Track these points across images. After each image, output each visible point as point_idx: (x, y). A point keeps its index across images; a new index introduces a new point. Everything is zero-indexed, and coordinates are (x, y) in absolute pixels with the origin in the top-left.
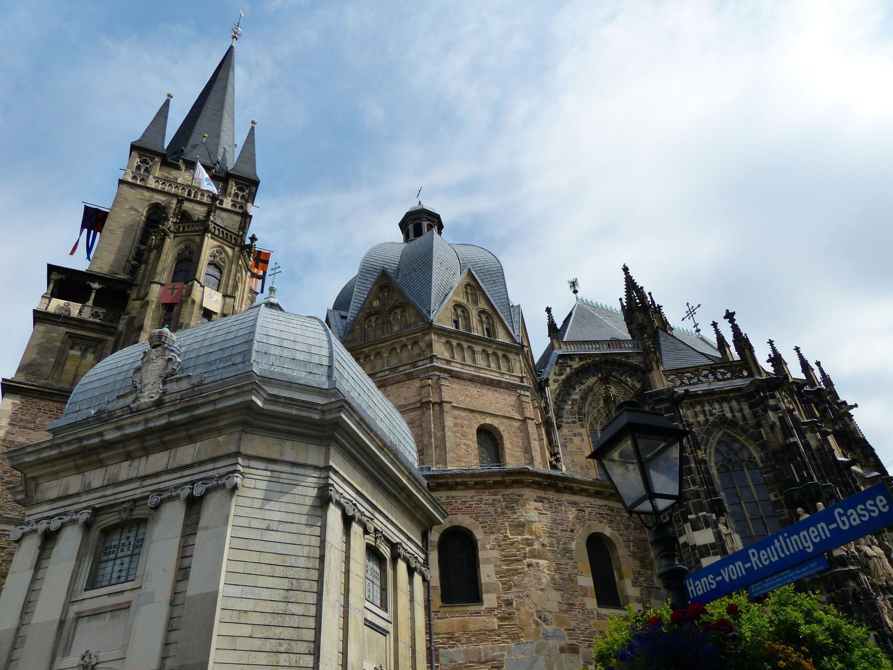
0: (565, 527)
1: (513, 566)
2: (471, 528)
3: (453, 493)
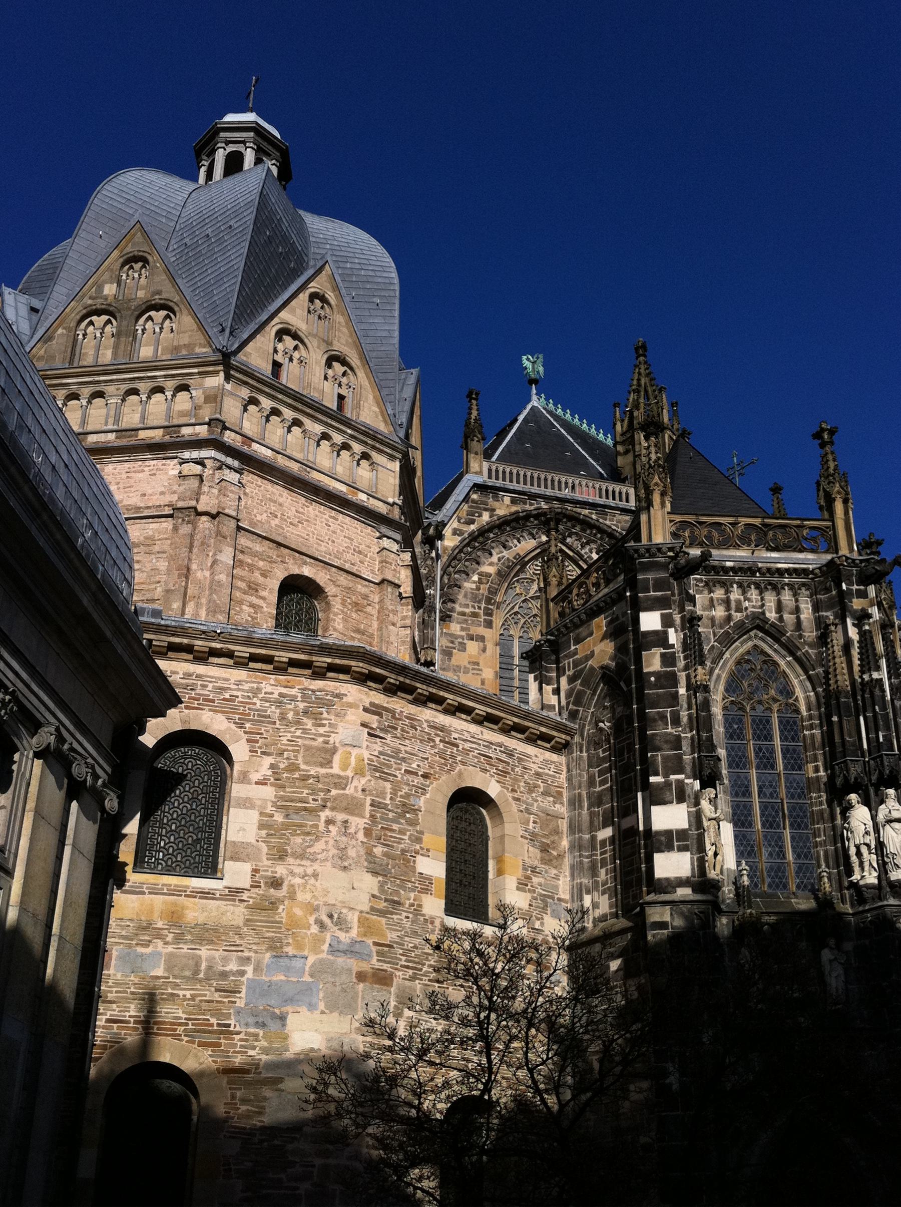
0: (414, 766)
1: (296, 819)
2: (226, 739)
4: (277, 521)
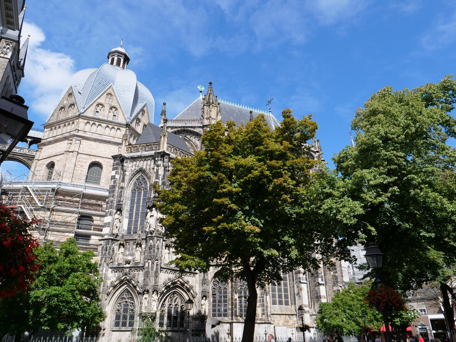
4: (90, 149)
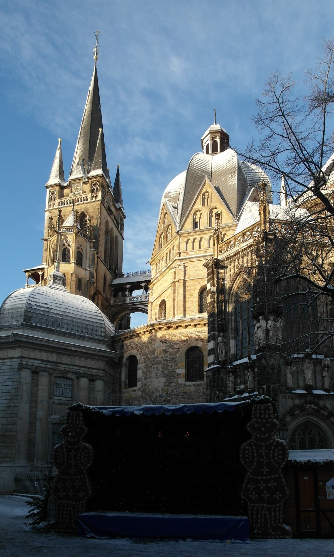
3: (131, 340)
4: (197, 272)
